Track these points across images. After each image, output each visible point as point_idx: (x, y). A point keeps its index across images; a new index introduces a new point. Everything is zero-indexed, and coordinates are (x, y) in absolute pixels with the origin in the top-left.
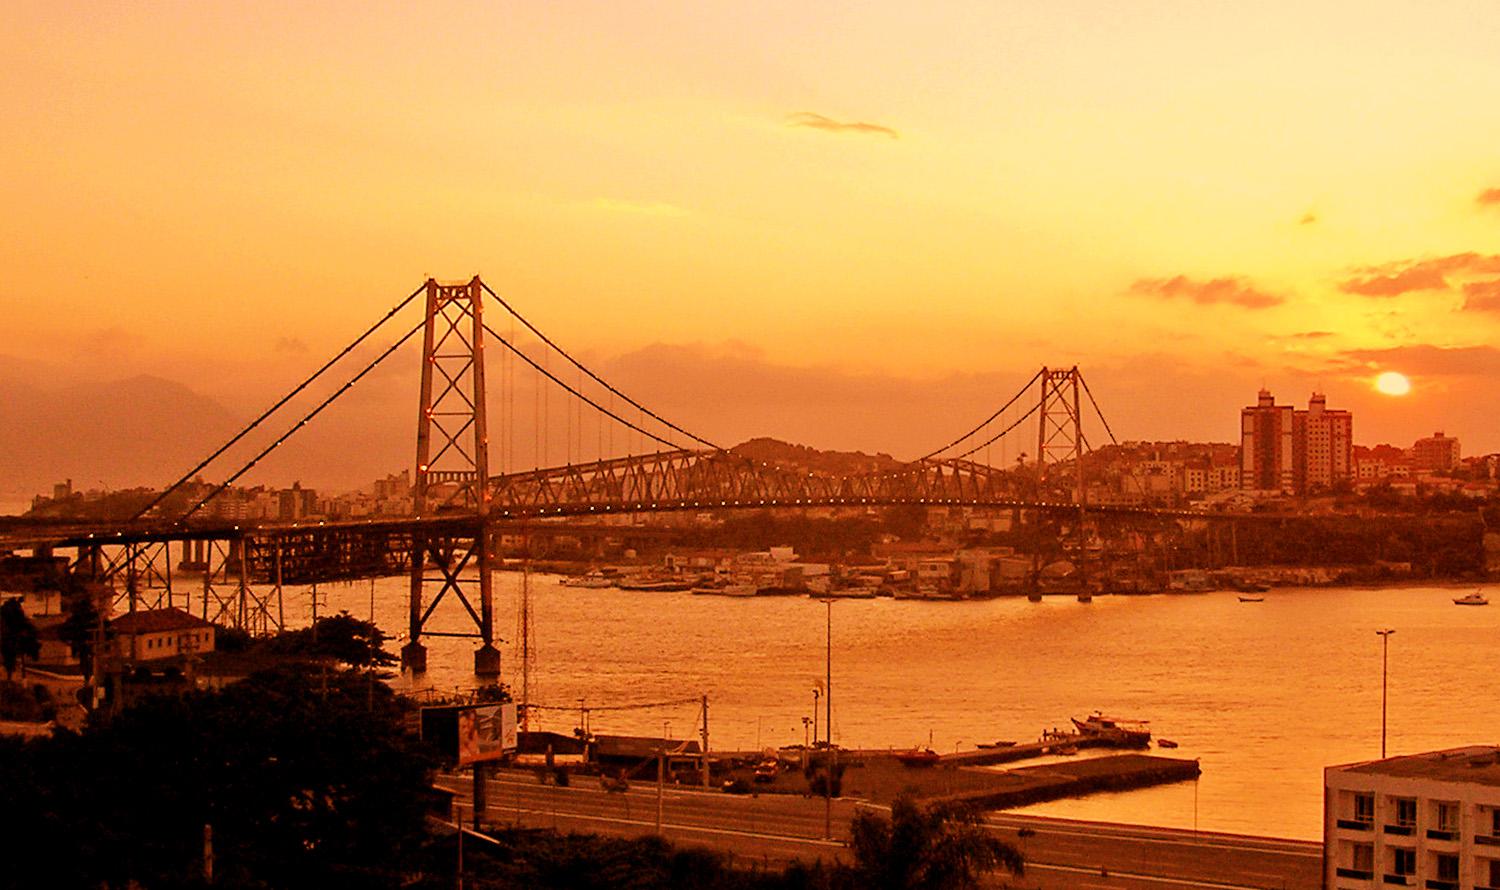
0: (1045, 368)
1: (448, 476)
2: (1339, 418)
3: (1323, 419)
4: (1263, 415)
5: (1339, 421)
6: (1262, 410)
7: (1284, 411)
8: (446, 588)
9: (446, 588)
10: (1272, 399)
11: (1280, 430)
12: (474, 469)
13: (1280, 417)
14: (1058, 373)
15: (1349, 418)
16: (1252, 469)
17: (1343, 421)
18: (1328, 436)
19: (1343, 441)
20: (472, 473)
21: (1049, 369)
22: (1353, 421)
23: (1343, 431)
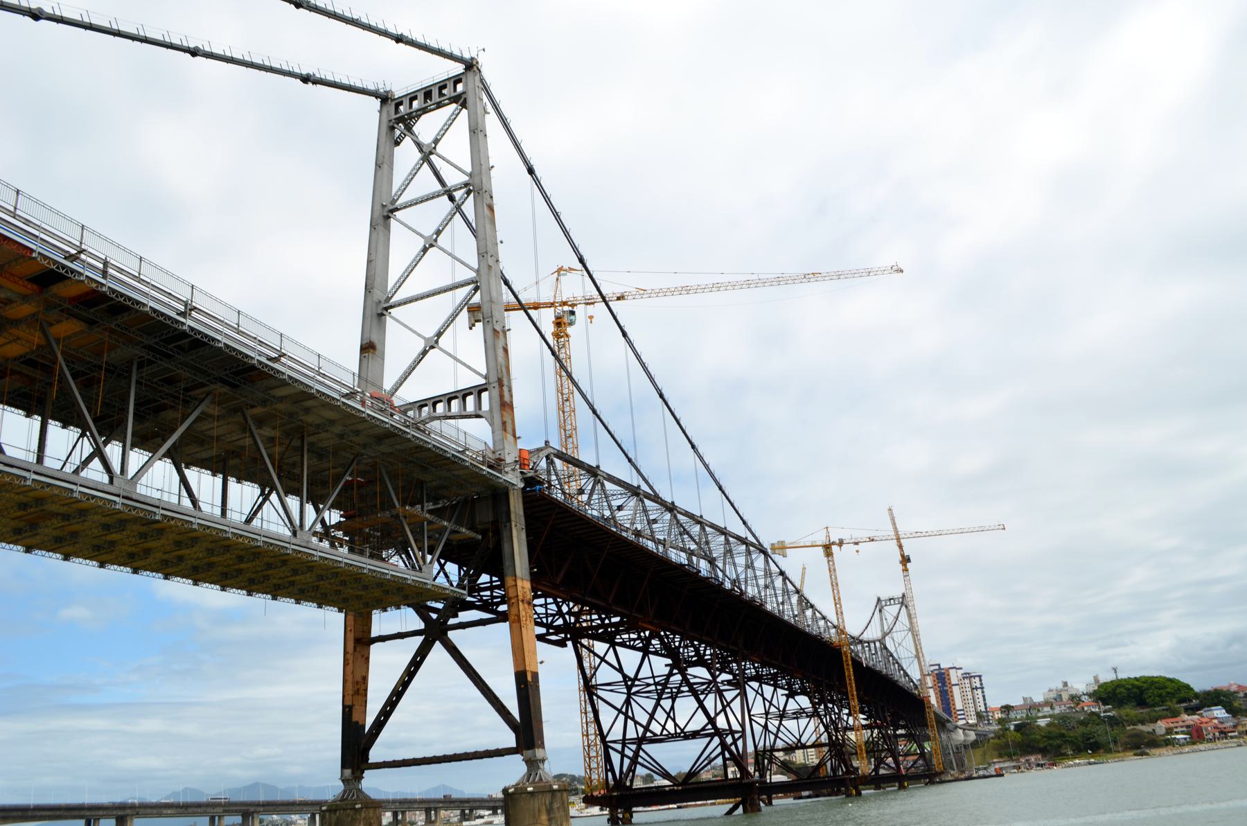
2: (974, 677)
3: (964, 678)
4: (937, 674)
6: (936, 672)
7: (950, 671)
8: (422, 653)
9: (422, 653)
10: (939, 665)
11: (950, 683)
13: (948, 675)
14: (890, 599)
15: (980, 676)
18: (970, 689)
19: (980, 691)
20: (480, 390)
21: (882, 599)
22: (982, 678)
23: (979, 686)
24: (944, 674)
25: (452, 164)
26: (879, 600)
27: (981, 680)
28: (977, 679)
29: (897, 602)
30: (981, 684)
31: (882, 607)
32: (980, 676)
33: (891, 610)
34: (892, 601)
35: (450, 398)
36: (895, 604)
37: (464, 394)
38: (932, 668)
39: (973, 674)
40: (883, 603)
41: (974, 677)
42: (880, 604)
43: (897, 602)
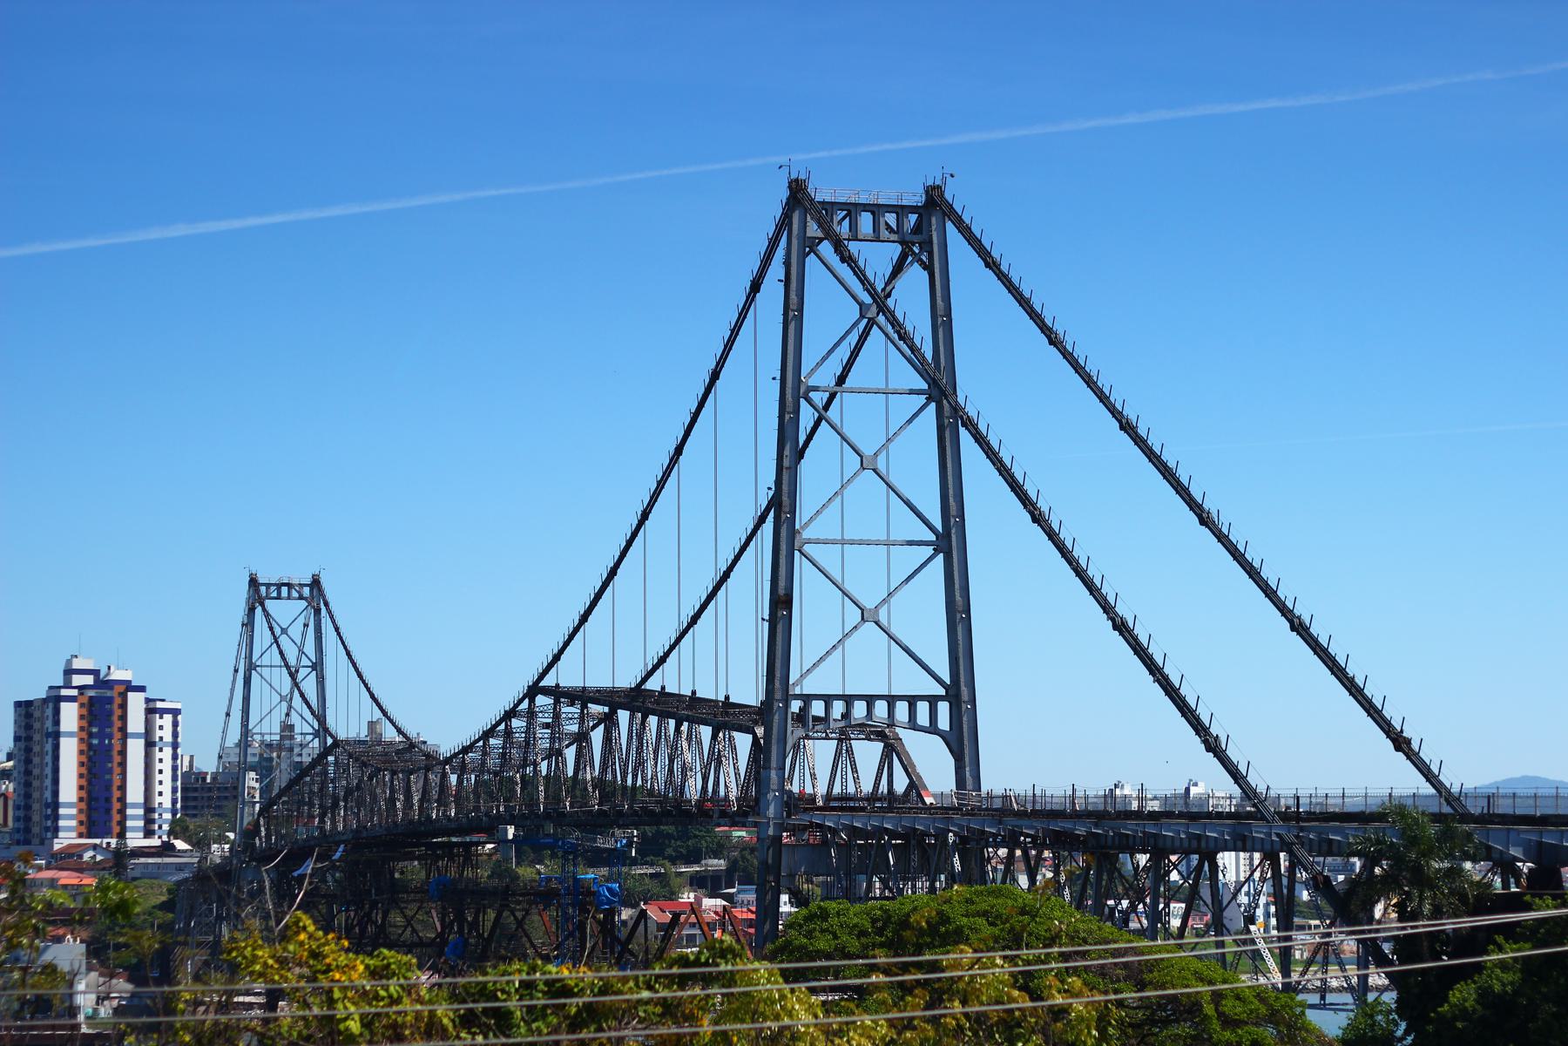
2: (163, 712)
5: (161, 717)
6: (92, 693)
12: (942, 692)
14: (279, 586)
16: (74, 799)
17: (168, 718)
19: (168, 751)
20: (933, 700)
23: (168, 738)
24: (110, 700)
26: (254, 582)
27: (175, 724)
28: (168, 718)
29: (295, 594)
30: (175, 735)
32: (175, 713)
33: (287, 611)
34: (284, 590)
36: (289, 598)
37: (912, 701)
38: (78, 680)
39: (159, 705)
40: (263, 589)
41: (163, 712)
42: (257, 594)
43: (295, 594)
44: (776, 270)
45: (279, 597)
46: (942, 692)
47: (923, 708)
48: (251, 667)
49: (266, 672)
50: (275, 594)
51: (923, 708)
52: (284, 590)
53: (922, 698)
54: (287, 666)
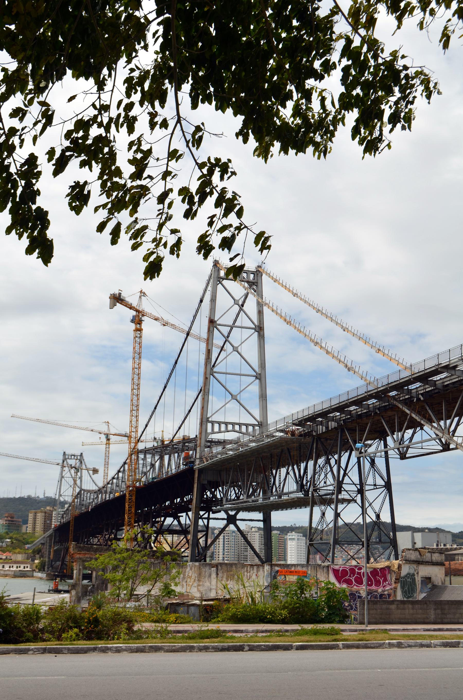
0: (64, 452)
1: (230, 427)
20: (253, 426)
21: (67, 453)
25: (248, 316)
29: (76, 458)
31: (66, 459)
34: (73, 457)
35: (240, 425)
37: (247, 425)
40: (67, 457)
44: (209, 288)
45: (71, 459)
46: (257, 423)
47: (250, 428)
48: (62, 477)
49: (65, 478)
50: (70, 458)
51: (250, 428)
52: (73, 457)
53: (250, 425)
54: (72, 477)
